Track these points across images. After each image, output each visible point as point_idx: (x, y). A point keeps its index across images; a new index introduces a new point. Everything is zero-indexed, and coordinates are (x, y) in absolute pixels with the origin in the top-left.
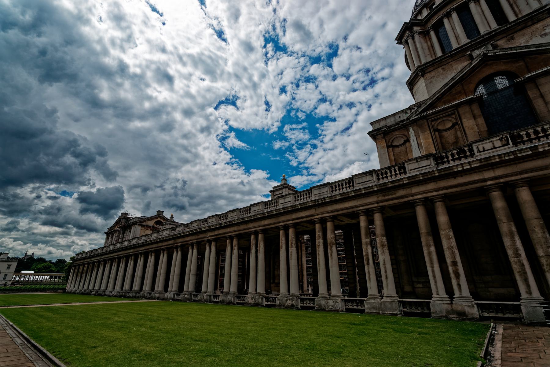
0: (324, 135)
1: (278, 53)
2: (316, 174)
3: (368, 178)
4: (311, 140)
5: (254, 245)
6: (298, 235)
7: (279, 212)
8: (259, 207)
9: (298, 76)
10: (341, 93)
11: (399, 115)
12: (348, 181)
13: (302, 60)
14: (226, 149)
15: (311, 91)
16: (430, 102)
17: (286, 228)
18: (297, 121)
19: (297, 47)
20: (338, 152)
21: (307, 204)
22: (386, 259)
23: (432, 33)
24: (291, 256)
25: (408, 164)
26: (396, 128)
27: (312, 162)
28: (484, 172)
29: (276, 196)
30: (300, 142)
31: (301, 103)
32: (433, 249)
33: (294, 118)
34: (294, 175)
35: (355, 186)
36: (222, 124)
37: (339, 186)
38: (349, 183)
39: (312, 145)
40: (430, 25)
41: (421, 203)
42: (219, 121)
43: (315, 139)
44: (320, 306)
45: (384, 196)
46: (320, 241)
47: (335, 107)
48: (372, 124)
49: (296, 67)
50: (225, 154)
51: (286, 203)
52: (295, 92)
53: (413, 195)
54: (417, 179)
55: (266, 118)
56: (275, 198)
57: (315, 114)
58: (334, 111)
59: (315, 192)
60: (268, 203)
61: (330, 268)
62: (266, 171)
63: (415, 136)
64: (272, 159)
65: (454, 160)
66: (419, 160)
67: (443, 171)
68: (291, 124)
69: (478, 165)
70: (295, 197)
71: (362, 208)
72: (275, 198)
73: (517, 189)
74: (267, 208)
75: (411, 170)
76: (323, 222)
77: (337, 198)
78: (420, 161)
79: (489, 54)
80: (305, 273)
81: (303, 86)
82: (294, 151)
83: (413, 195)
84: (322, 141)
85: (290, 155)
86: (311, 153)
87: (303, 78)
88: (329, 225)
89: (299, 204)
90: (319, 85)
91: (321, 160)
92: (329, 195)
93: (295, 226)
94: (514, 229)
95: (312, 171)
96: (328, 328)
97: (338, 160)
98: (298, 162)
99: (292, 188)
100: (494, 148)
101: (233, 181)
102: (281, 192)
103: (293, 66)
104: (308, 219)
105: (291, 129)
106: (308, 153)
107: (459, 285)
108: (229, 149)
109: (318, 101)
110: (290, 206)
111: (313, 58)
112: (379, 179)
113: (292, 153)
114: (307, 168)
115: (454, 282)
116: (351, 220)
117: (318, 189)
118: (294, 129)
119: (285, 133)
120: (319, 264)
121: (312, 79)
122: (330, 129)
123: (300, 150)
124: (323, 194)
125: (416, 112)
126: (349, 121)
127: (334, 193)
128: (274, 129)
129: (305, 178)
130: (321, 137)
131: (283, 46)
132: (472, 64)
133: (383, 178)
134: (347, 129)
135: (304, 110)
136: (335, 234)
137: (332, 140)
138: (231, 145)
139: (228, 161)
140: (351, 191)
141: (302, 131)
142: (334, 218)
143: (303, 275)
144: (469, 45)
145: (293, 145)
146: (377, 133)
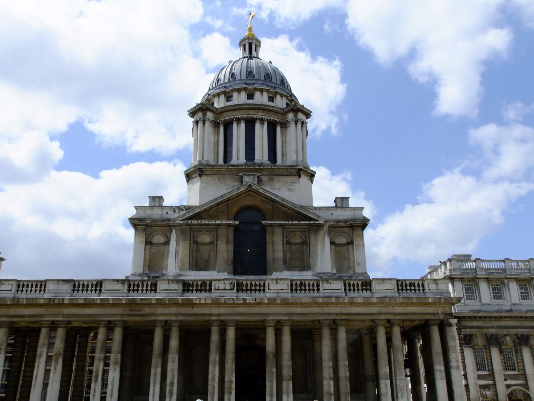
3: (119, 286)
25: (160, 284)
28: (213, 308)
35: (102, 291)
38: (96, 286)
40: (222, 120)
45: (131, 310)
48: (136, 208)
63: (176, 241)
65: (197, 290)
66: (170, 282)
69: (211, 302)
75: (161, 290)
78: (171, 284)
94: (217, 359)
100: (225, 290)
112: (129, 290)
117: (55, 284)
120: (36, 378)
124: (61, 292)
125: (182, 218)
132: (239, 190)
133: (134, 290)
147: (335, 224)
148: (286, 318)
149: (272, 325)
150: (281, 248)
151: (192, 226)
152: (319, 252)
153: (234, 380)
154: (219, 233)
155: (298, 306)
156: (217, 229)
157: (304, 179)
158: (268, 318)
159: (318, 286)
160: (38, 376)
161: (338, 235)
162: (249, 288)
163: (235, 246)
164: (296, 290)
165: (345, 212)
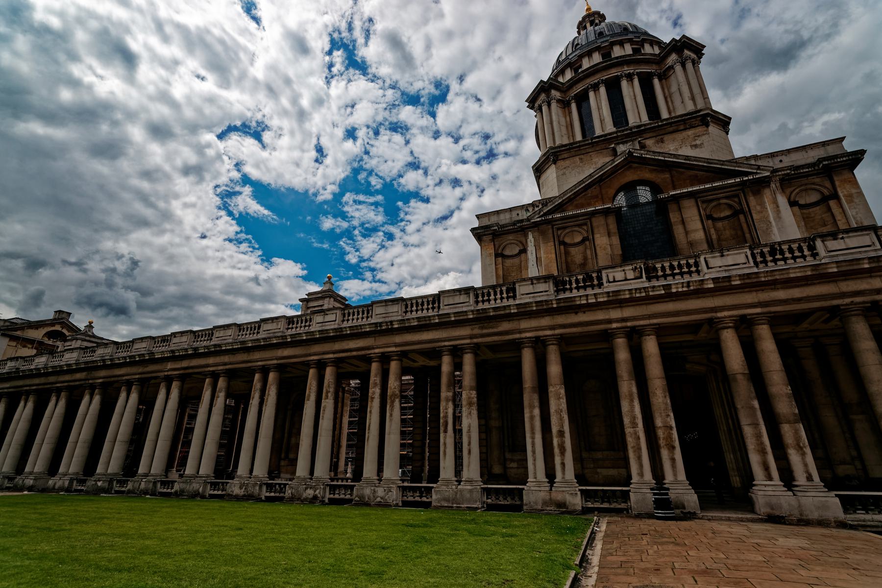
0: (407, 221)
1: (351, 70)
2: (386, 281)
3: (463, 298)
4: (386, 226)
5: (258, 391)
6: (341, 379)
7: (313, 337)
8: (278, 325)
9: (380, 118)
10: (444, 161)
11: (517, 212)
12: (431, 299)
13: (390, 92)
14: (230, 214)
15: (397, 147)
16: (560, 201)
17: (321, 366)
18: (368, 190)
19: (384, 71)
20: (426, 251)
21: (361, 329)
22: (472, 425)
23: (574, 106)
24: (324, 413)
25: (520, 286)
26: (511, 229)
27: (383, 261)
28: (610, 310)
29: (311, 310)
30: (367, 225)
31: (379, 162)
32: (537, 412)
33: (363, 184)
34: (348, 278)
35: (441, 307)
36: (228, 167)
37: (417, 306)
38: (433, 303)
39: (385, 233)
40: (573, 95)
41: (530, 344)
42: (223, 161)
43: (392, 224)
44: (362, 497)
45: (482, 328)
46: (375, 392)
47: (430, 181)
48: (478, 217)
49: (378, 101)
50: (227, 222)
51: (327, 324)
52: (371, 142)
53: (520, 331)
54: (528, 309)
55: (314, 175)
56: (309, 312)
57: (399, 184)
58: (428, 186)
59: (378, 310)
60: (295, 320)
61: (386, 436)
62: (301, 264)
64: (315, 245)
65: (578, 288)
66: (535, 282)
67: (563, 302)
68: (357, 193)
69: (605, 299)
70: (344, 316)
71: (447, 343)
72: (309, 312)
73: (644, 337)
74: (292, 328)
75: (523, 295)
76: (385, 359)
77: (412, 324)
79: (634, 154)
80: (344, 443)
81: (385, 135)
82: (355, 238)
83: (520, 331)
84: (403, 231)
85: (347, 244)
86: (383, 247)
87: (387, 123)
88: (394, 366)
89: (350, 327)
90: (411, 141)
91: (398, 261)
92: (400, 318)
93: (337, 363)
94: (634, 390)
95: (380, 276)
96: (369, 533)
97: (424, 265)
98: (359, 257)
99: (342, 300)
100: (626, 280)
101: (236, 272)
102: (320, 303)
103: (373, 99)
104: (360, 353)
105: (355, 201)
106: (378, 245)
107: (563, 464)
108: (237, 216)
109: (407, 166)
110: (332, 329)
111: (407, 95)
112: (477, 302)
113: (351, 242)
114: (373, 270)
115: (558, 460)
116: (428, 361)
118: (360, 203)
119: (343, 206)
120: (369, 429)
121: (401, 128)
122: (418, 213)
123: (365, 238)
124: (391, 315)
125: (539, 213)
126: (449, 206)
127: (409, 316)
128: (326, 195)
129: (367, 285)
130: (403, 224)
131: (362, 62)
132: (614, 162)
133: (483, 301)
134: (445, 218)
135: (381, 174)
136: (401, 380)
137: (418, 231)
138: (241, 208)
139: (232, 236)
140: (434, 316)
141: (373, 207)
142: (403, 355)
143: (339, 446)
144: (615, 135)
145: (355, 228)
146: (485, 232)
147: (793, 172)
148: (758, 310)
149: (730, 325)
150: (699, 225)
151: (554, 223)
152: (772, 219)
153: (673, 424)
154: (594, 224)
155: (779, 286)
156: (590, 219)
157: (713, 129)
158: (719, 315)
159: (812, 248)
160: (371, 425)
161: (801, 191)
162: (668, 272)
163: (622, 240)
164: (765, 262)
165: (807, 152)
